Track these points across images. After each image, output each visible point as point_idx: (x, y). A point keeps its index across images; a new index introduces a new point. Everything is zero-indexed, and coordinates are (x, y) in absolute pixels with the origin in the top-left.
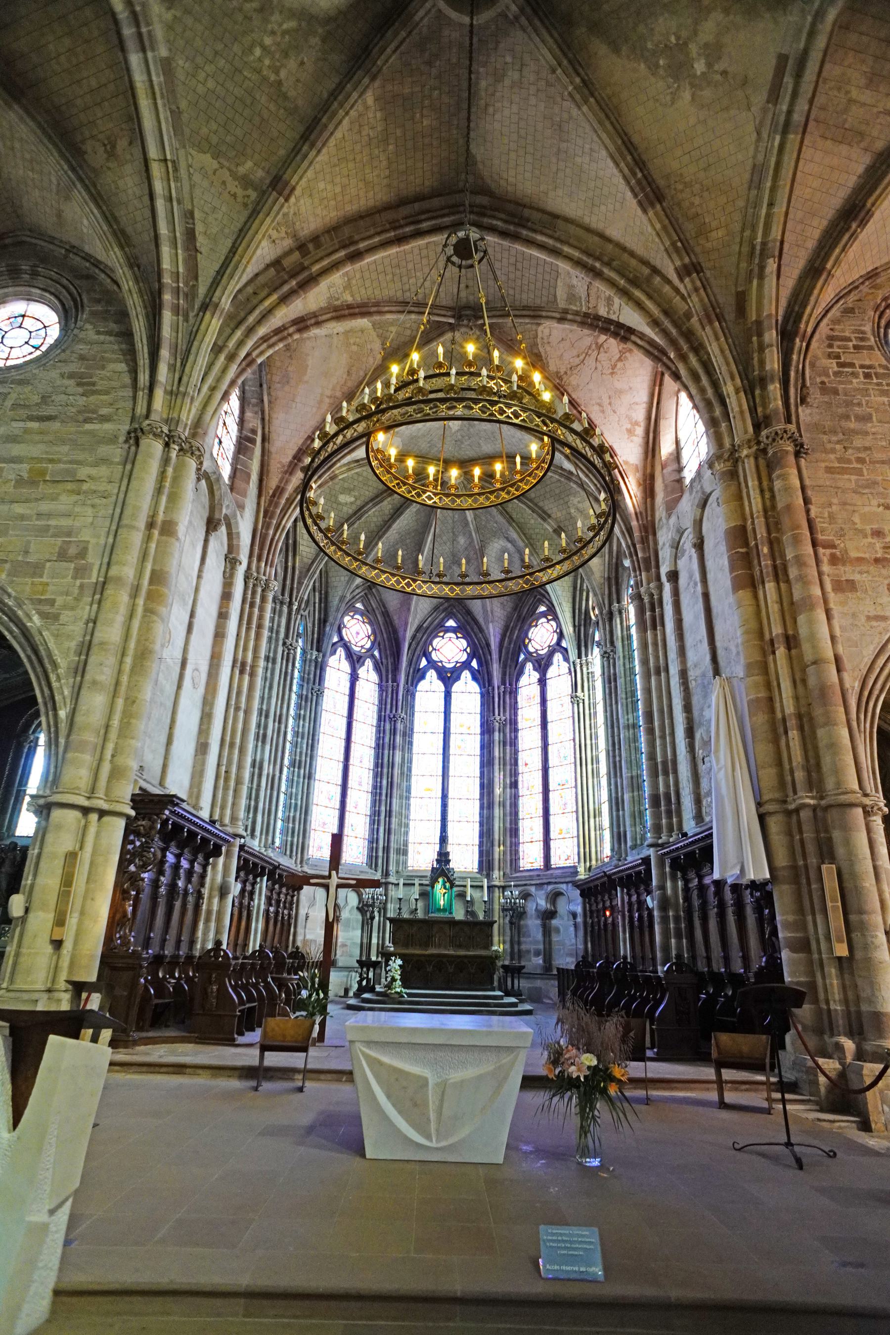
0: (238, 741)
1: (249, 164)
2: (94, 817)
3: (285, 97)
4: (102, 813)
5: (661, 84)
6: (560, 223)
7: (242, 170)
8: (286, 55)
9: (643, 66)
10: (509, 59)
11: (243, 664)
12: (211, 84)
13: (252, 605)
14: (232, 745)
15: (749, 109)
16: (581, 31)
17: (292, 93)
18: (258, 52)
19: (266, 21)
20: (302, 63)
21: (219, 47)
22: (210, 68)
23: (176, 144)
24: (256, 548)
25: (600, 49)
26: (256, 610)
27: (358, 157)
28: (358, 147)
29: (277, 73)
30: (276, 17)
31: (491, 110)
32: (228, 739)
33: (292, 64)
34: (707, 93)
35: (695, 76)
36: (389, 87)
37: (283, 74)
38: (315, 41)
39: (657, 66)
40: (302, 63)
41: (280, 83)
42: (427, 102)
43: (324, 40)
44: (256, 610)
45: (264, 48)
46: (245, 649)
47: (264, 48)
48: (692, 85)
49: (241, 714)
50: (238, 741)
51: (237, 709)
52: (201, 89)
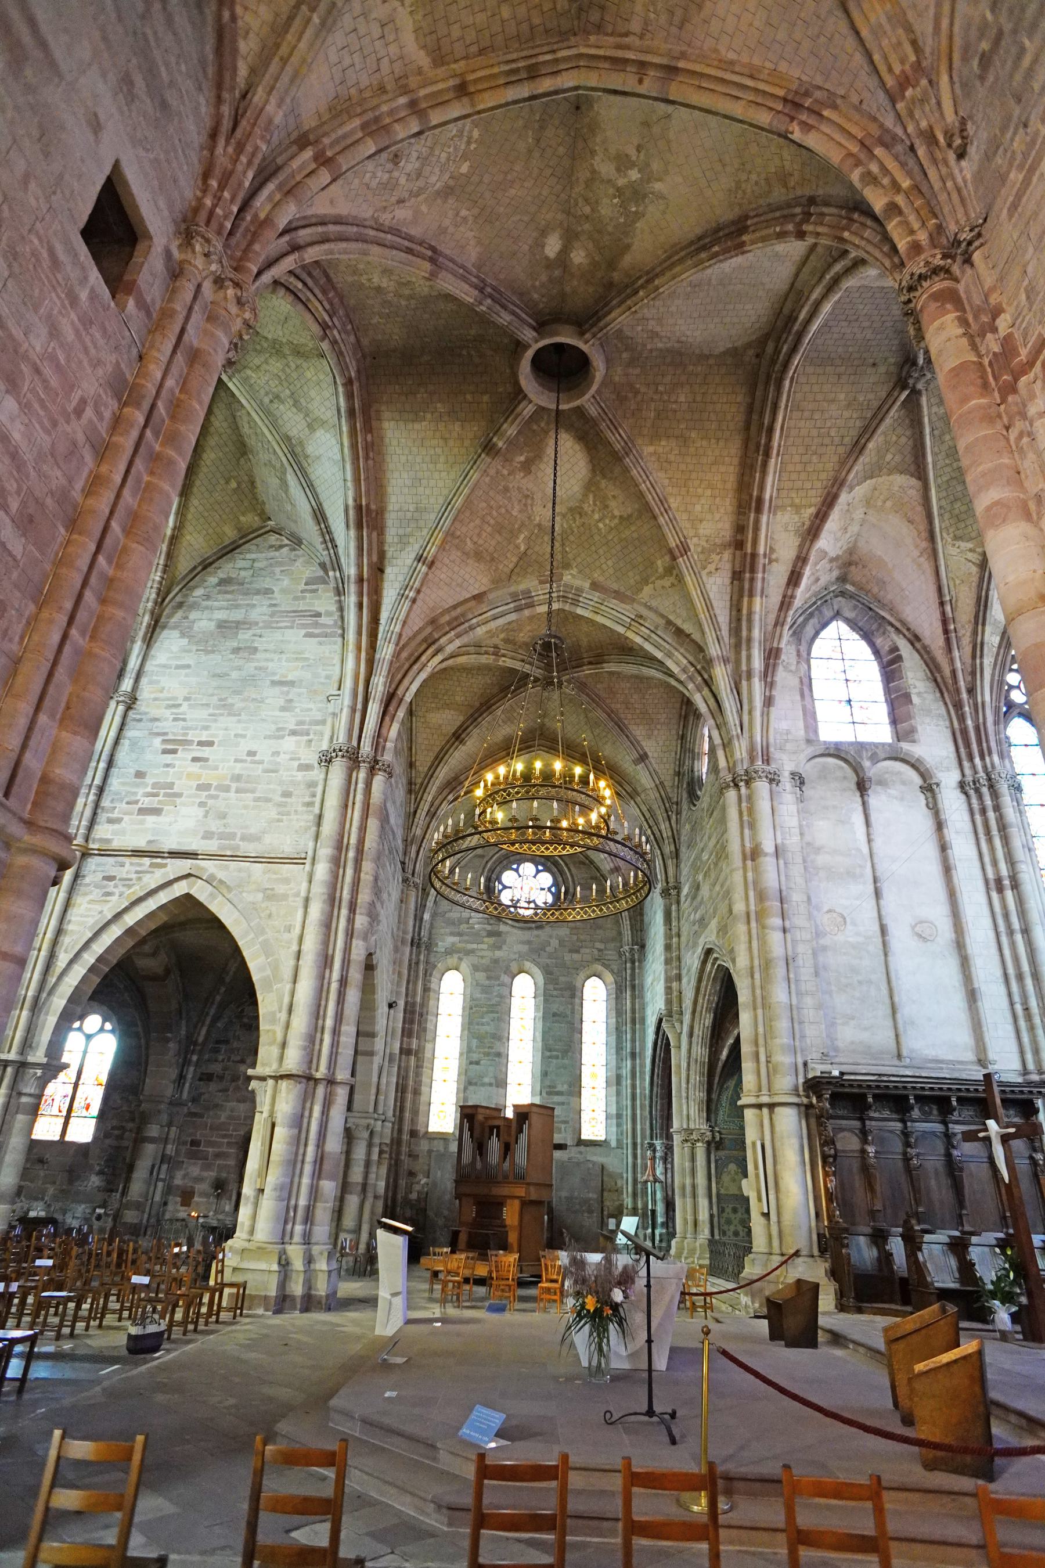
0: (1026, 967)
1: (659, 563)
2: (765, 1111)
3: (630, 516)
4: (771, 1106)
5: (651, 208)
6: (798, 285)
7: (661, 570)
8: (607, 506)
9: (638, 225)
10: (640, 328)
11: (999, 881)
12: (610, 563)
13: (983, 811)
14: (1020, 977)
15: (669, 116)
17: (629, 511)
18: (601, 525)
19: (586, 514)
20: (614, 497)
21: (593, 548)
22: (603, 560)
23: (628, 607)
24: (962, 750)
25: (627, 260)
26: (991, 815)
27: (691, 467)
28: (683, 467)
29: (614, 517)
30: (585, 506)
31: (684, 339)
32: (1011, 971)
33: (613, 504)
34: (656, 166)
35: (641, 179)
36: (645, 431)
37: (616, 513)
38: (603, 483)
39: (636, 213)
40: (614, 497)
42: (666, 397)
43: (604, 477)
44: (991, 815)
45: (600, 520)
46: (995, 863)
47: (600, 520)
48: (649, 181)
49: (1019, 938)
50: (1026, 967)
51: (1011, 932)
52: (611, 571)
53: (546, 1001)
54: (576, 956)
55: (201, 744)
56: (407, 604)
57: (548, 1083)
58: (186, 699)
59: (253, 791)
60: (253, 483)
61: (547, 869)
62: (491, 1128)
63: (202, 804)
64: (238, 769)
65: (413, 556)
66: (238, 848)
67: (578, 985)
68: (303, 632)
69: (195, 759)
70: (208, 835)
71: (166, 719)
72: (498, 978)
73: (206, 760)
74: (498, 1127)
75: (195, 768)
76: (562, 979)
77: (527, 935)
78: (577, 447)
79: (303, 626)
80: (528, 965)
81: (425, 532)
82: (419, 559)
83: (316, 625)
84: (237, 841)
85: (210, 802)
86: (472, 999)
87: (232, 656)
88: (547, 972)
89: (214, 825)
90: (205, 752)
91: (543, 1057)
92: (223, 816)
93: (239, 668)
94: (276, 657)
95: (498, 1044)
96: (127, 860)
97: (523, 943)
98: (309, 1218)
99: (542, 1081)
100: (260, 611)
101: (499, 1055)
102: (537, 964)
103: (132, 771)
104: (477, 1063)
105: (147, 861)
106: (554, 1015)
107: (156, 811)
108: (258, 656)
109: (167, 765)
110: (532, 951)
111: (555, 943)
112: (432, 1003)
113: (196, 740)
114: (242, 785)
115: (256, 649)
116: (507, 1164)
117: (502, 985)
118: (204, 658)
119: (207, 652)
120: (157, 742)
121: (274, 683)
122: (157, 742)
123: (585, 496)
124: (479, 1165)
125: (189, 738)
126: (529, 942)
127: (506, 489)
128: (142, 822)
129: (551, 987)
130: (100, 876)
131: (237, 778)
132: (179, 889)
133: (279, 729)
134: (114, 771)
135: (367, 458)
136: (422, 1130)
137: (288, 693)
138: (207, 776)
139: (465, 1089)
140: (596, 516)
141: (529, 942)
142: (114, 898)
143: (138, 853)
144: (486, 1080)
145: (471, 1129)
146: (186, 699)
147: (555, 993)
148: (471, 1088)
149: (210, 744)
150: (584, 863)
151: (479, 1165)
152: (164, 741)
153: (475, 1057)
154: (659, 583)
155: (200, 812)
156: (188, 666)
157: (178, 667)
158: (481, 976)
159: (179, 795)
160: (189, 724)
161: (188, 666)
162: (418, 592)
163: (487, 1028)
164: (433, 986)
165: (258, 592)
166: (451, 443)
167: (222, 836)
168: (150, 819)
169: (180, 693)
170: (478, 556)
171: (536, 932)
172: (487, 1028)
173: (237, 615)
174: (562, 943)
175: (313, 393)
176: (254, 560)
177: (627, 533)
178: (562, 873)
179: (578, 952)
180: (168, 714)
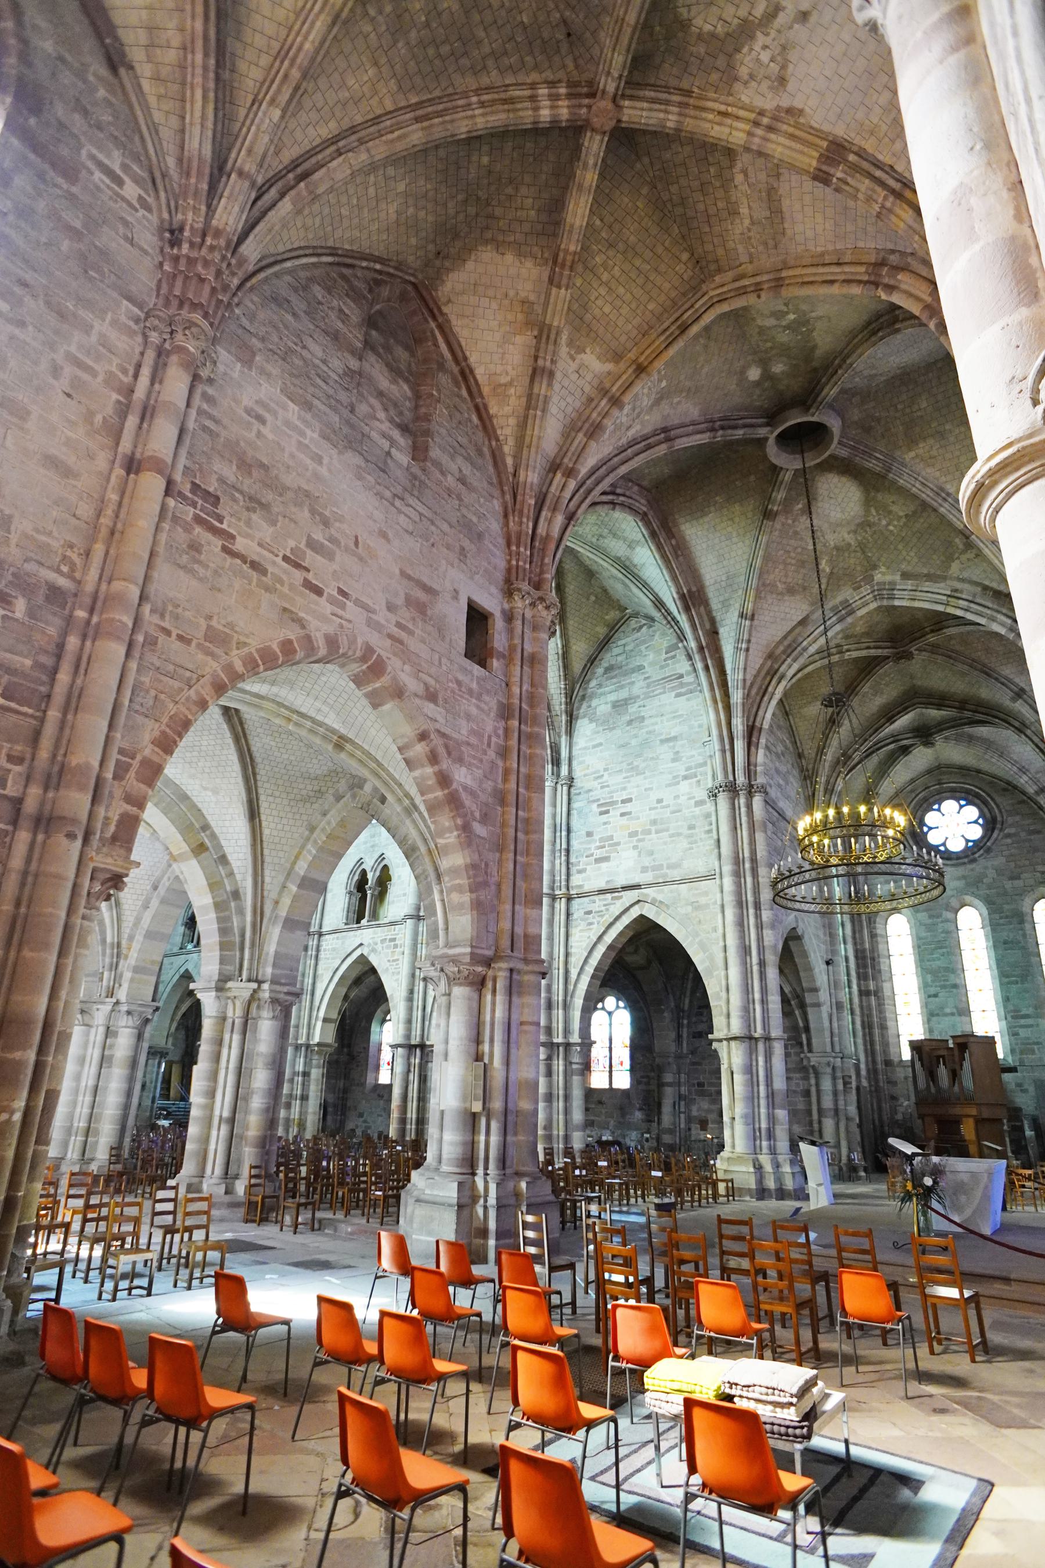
7: (961, 546)
8: (890, 512)
12: (912, 554)
16: (815, 364)
18: (891, 528)
19: (874, 524)
22: (904, 553)
23: (942, 585)
25: (818, 353)
27: (957, 453)
28: (948, 456)
30: (871, 519)
33: (894, 508)
36: (901, 443)
37: (901, 514)
38: (879, 496)
41: (906, 516)
43: (878, 491)
45: (888, 524)
47: (888, 524)
52: (916, 560)
53: (993, 930)
54: (1018, 883)
55: (623, 802)
56: (743, 654)
57: (1011, 1007)
58: (606, 770)
59: (667, 830)
60: (605, 591)
61: (969, 803)
62: (938, 1057)
63: (635, 847)
64: (653, 815)
65: (736, 614)
66: (666, 875)
67: (1026, 909)
68: (673, 694)
69: (622, 815)
70: (644, 870)
72: (940, 916)
73: (630, 813)
74: (943, 1057)
75: (624, 821)
76: (1006, 907)
77: (960, 871)
78: (844, 479)
79: (673, 689)
80: (968, 898)
81: (740, 592)
82: (742, 615)
83: (682, 685)
84: (665, 871)
85: (640, 844)
86: (919, 938)
88: (989, 902)
89: (647, 861)
90: (628, 807)
91: (1001, 984)
92: (651, 853)
93: (636, 736)
94: (658, 720)
95: (952, 976)
96: (596, 898)
97: (959, 879)
98: (771, 1135)
99: (1005, 1007)
100: (638, 686)
101: (955, 986)
102: (976, 896)
103: (584, 833)
104: (936, 996)
105: (609, 896)
106: (1005, 942)
107: (606, 859)
108: (646, 722)
109: (605, 823)
110: (968, 885)
111: (991, 873)
112: (881, 947)
114: (659, 827)
115: (643, 718)
116: (956, 1088)
117: (947, 921)
118: (609, 734)
119: (611, 729)
120: (594, 806)
121: (662, 741)
122: (594, 806)
123: (867, 512)
124: (933, 1090)
126: (964, 877)
127: (796, 533)
128: (599, 869)
129: (997, 916)
130: (582, 912)
131: (654, 822)
132: (635, 913)
133: (675, 777)
134: (572, 835)
135: (677, 556)
136: (896, 1060)
137: (674, 747)
138: (635, 825)
139: (929, 1021)
140: (884, 522)
141: (964, 877)
142: (595, 926)
143: (602, 892)
144: (948, 1010)
145: (920, 1059)
146: (606, 770)
147: (1002, 921)
148: (934, 1019)
149: (630, 800)
150: (1005, 790)
151: (933, 1090)
152: (599, 806)
153: (932, 991)
154: (964, 557)
155: (635, 853)
156: (601, 744)
157: (594, 747)
158: (923, 916)
159: (618, 844)
161: (601, 744)
162: (749, 641)
163: (938, 963)
164: (879, 931)
165: (633, 671)
166: (737, 520)
167: (654, 868)
168: (604, 865)
169: (600, 766)
170: (791, 591)
171: (970, 867)
172: (938, 963)
173: (623, 694)
174: (999, 872)
175: (624, 526)
177: (918, 525)
178: (985, 803)
179: (1018, 878)
180: (596, 784)
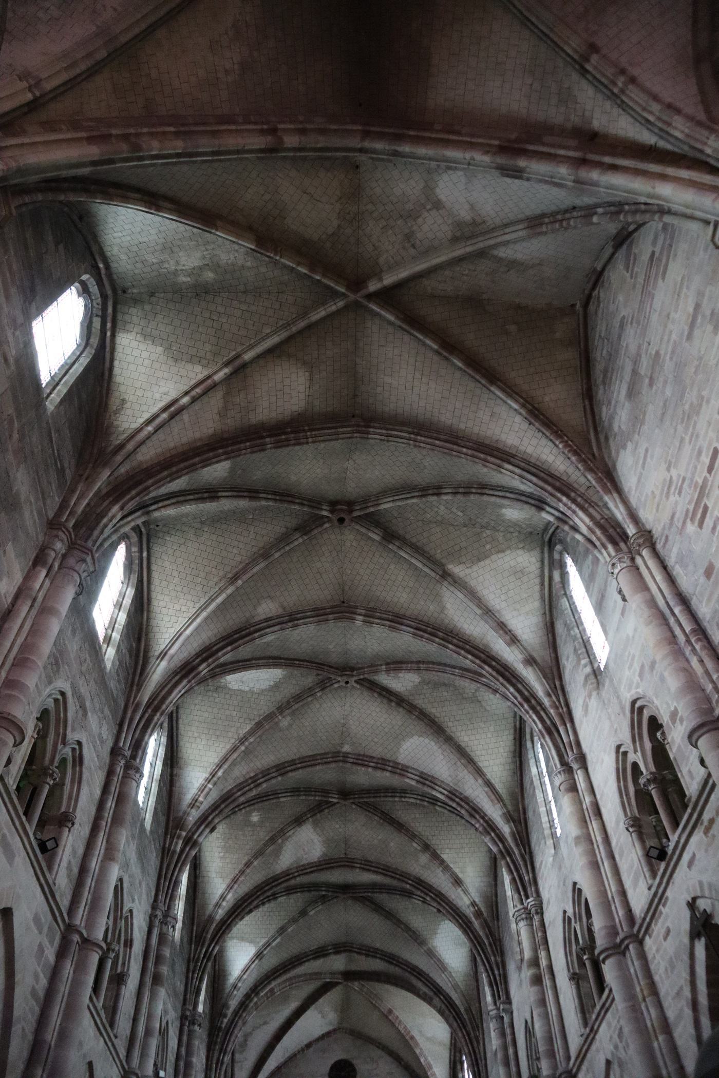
56: (633, 91)
58: (668, 469)
68: (660, 281)
71: (676, 503)
83: (660, 260)
87: (655, 388)
103: (702, 579)
108: (662, 352)
113: (705, 473)
121: (690, 337)
125: (700, 482)
134: (694, 602)
152: (692, 520)
160: (689, 475)
161: (647, 450)
162: (623, 72)
176: (600, 336)
